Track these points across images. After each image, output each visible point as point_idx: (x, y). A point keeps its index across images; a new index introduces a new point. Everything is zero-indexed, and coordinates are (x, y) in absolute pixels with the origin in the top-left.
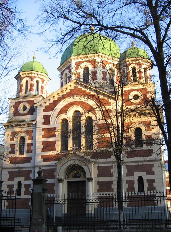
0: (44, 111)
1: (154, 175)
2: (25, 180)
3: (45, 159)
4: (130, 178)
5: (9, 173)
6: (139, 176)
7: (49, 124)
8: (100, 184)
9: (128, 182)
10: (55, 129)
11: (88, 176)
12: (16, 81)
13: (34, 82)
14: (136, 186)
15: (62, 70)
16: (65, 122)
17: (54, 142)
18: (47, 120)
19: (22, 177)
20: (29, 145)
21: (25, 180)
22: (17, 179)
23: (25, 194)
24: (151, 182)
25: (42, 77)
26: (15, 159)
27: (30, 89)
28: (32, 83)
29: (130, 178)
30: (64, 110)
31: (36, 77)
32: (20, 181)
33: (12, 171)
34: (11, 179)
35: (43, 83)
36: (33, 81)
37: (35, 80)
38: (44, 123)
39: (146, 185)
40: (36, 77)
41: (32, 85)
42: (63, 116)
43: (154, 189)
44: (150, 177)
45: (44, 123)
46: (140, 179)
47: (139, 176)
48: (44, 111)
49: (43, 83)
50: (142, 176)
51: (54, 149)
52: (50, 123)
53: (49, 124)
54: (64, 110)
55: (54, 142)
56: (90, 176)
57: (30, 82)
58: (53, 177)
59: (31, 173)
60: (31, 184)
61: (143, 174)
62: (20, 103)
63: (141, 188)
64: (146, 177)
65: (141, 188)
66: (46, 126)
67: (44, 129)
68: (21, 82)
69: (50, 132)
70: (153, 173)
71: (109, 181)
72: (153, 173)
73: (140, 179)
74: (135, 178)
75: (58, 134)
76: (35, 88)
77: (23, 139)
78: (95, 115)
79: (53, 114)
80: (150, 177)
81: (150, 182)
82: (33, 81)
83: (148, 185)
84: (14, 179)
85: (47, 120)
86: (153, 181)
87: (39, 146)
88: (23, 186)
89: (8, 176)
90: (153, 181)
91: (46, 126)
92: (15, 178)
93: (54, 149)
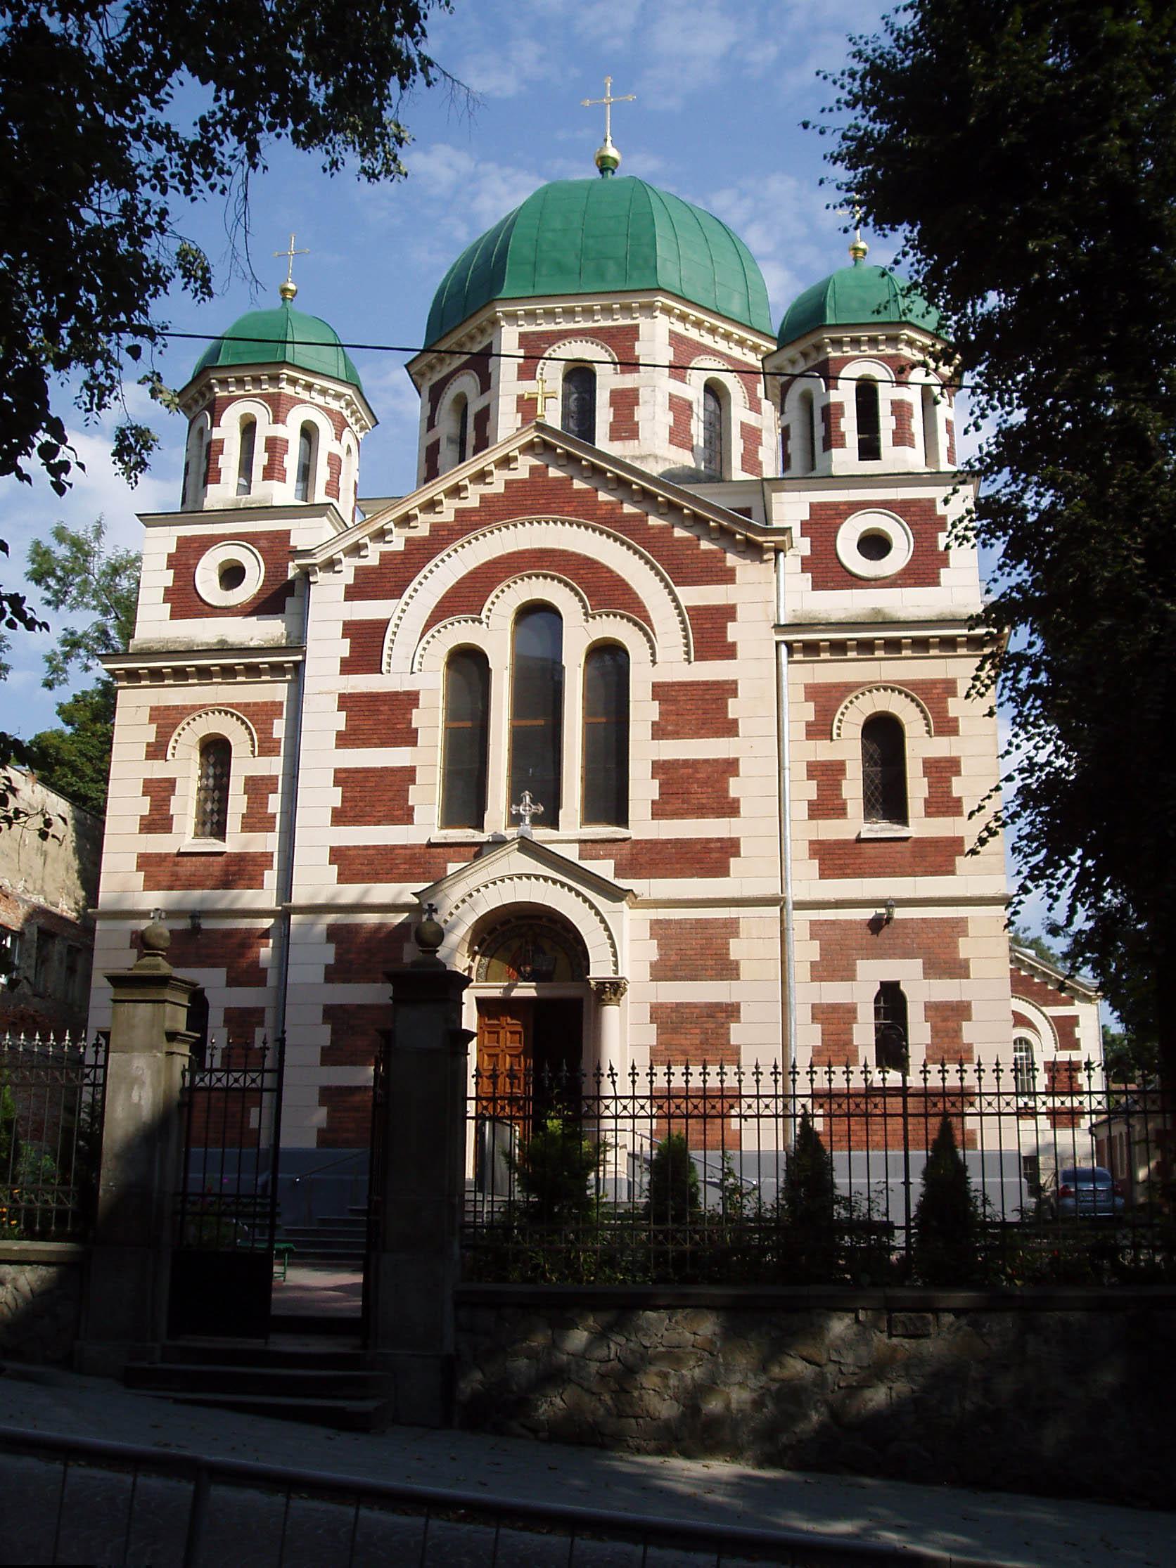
0: (353, 593)
1: (968, 977)
2: (232, 982)
3: (351, 864)
4: (835, 992)
6: (882, 983)
7: (374, 666)
8: (668, 1019)
9: (822, 1013)
10: (411, 699)
11: (599, 969)
12: (182, 420)
13: (290, 431)
14: (864, 1036)
15: (437, 377)
16: (468, 665)
17: (408, 775)
18: (366, 645)
20: (258, 787)
21: (232, 982)
24: (949, 1016)
25: (335, 405)
27: (265, 468)
28: (279, 431)
29: (835, 992)
30: (466, 598)
31: (303, 402)
35: (339, 437)
36: (284, 422)
37: (297, 417)
38: (348, 667)
39: (919, 1034)
40: (303, 402)
41: (274, 446)
42: (460, 632)
43: (962, 1056)
44: (946, 990)
45: (348, 667)
46: (891, 1000)
47: (882, 983)
48: (353, 593)
49: (339, 437)
50: (897, 984)
51: (406, 816)
52: (384, 668)
53: (374, 666)
54: (466, 598)
55: (408, 775)
56: (616, 972)
57: (265, 430)
60: (262, 1010)
61: (907, 972)
62: (207, 543)
63: (892, 1050)
64: (920, 992)
65: (892, 1050)
67: (345, 701)
68: (216, 423)
69: (378, 718)
70: (959, 970)
71: (718, 1005)
72: (959, 970)
73: (891, 1000)
74: (860, 993)
75: (431, 720)
76: (292, 462)
77: (216, 751)
78: (646, 634)
79: (406, 614)
80: (946, 990)
81: (945, 1020)
82: (284, 422)
83: (935, 1031)
85: (366, 645)
86: (961, 1011)
88: (215, 1018)
90: (961, 1011)
93: (406, 816)
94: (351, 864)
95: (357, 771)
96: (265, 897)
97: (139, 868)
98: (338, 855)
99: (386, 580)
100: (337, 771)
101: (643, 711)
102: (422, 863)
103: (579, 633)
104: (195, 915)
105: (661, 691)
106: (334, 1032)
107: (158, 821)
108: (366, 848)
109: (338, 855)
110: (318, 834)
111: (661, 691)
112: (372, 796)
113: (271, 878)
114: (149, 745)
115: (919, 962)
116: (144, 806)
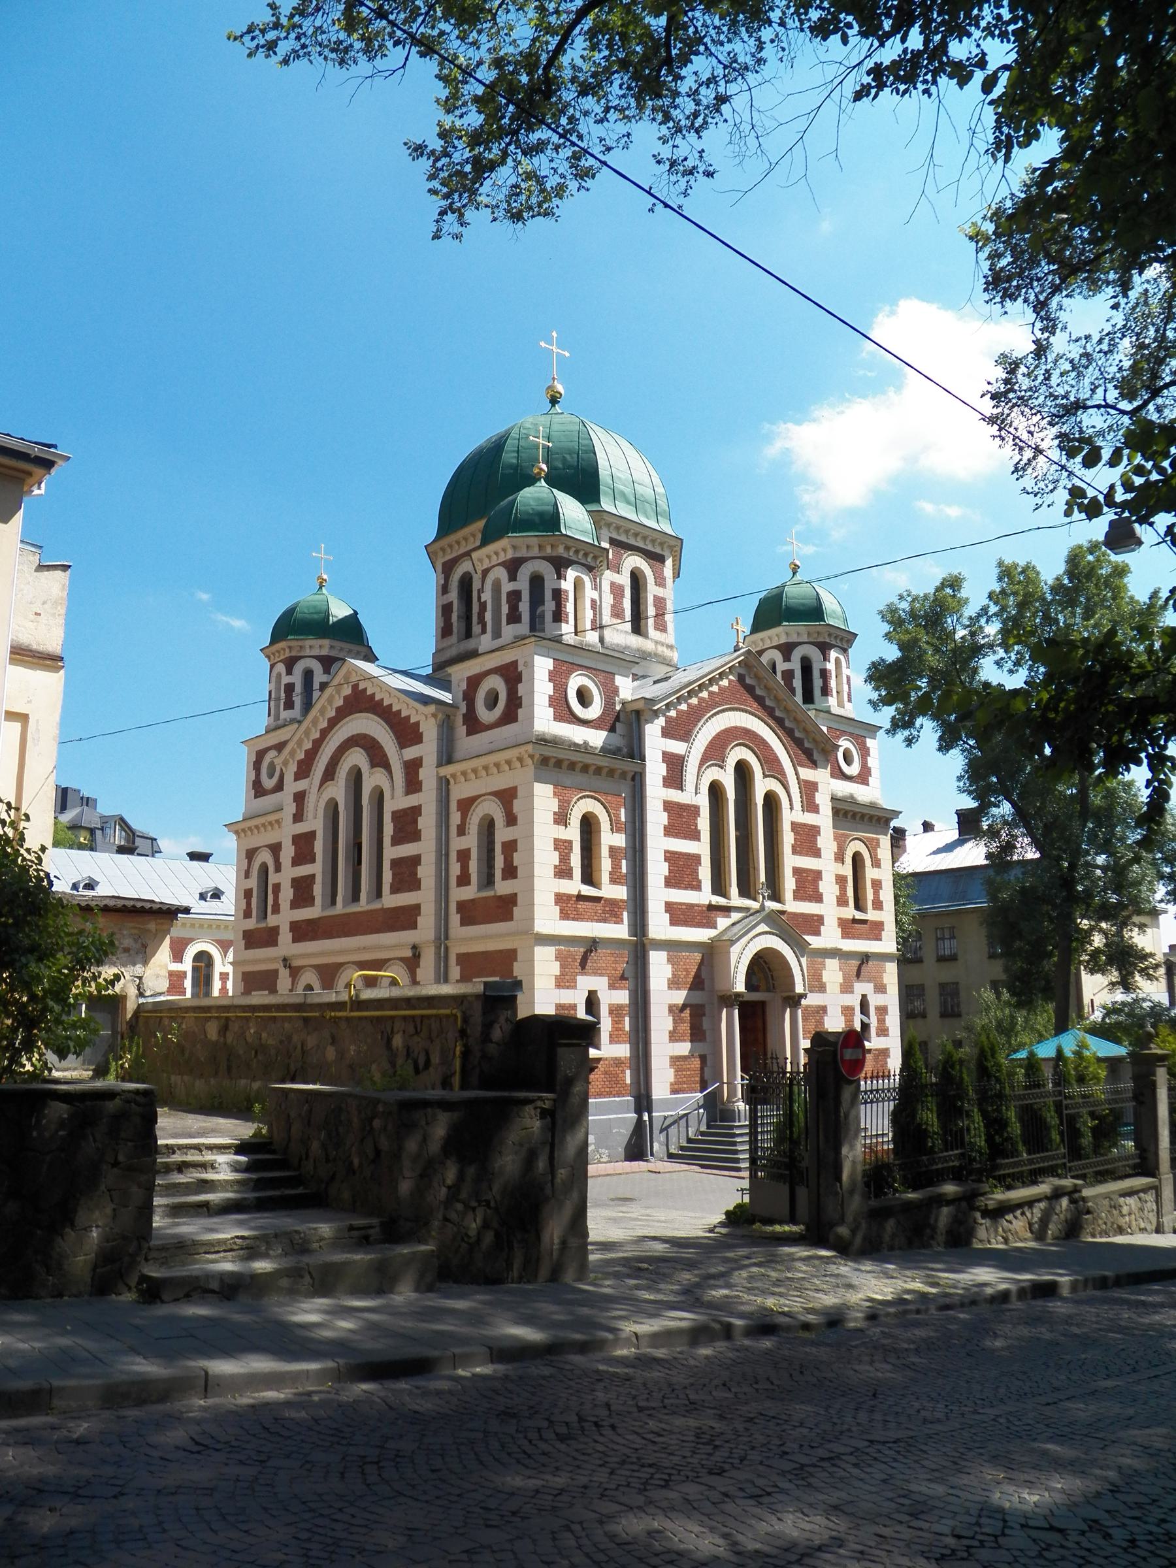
3: (679, 915)
19: (601, 975)
42: (712, 774)
51: (698, 887)
64: (874, 1000)
66: (674, 795)
67: (669, 806)
69: (681, 820)
74: (854, 1001)
89: (555, 968)
91: (674, 795)
92: (579, 978)
94: (679, 915)
95: (676, 853)
98: (670, 907)
99: (680, 729)
100: (666, 852)
101: (788, 838)
103: (762, 785)
105: (795, 826)
107: (563, 872)
109: (670, 907)
111: (795, 826)
112: (681, 871)
114: (555, 813)
115: (872, 985)
116: (555, 858)
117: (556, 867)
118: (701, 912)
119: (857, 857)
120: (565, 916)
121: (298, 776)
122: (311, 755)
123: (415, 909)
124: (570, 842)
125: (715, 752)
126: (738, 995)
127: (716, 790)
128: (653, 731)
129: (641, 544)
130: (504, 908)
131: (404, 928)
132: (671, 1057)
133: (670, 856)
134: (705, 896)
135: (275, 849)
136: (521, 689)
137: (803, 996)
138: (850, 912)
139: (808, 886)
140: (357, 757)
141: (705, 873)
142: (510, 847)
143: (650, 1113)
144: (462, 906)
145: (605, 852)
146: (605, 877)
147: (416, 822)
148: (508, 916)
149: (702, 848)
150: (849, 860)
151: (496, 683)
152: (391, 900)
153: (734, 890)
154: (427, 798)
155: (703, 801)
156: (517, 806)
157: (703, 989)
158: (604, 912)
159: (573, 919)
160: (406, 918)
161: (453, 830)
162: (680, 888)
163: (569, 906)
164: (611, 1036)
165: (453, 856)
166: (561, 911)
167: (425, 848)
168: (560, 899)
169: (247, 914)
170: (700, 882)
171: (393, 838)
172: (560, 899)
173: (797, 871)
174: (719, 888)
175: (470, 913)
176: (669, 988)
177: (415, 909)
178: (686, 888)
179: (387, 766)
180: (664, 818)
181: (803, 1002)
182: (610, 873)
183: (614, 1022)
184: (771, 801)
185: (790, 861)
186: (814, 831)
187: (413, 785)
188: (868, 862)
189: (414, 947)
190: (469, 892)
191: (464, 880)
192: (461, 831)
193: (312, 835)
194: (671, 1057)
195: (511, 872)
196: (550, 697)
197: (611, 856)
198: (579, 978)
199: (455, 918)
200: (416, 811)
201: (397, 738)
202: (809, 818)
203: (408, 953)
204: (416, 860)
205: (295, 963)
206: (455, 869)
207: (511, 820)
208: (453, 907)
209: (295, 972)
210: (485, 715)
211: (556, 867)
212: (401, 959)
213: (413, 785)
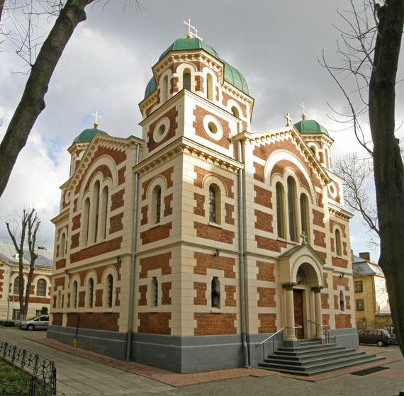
2: (226, 276)
3: (262, 242)
5: (197, 255)
19: (221, 269)
21: (226, 276)
22: (212, 273)
23: (227, 304)
26: (207, 229)
32: (217, 278)
33: (202, 253)
34: (199, 270)
42: (277, 178)
51: (271, 231)
58: (272, 279)
59: (234, 264)
74: (338, 293)
84: (206, 271)
87: (251, 219)
91: (259, 184)
92: (208, 269)
94: (262, 242)
95: (260, 212)
96: (234, 247)
97: (195, 227)
98: (257, 238)
101: (311, 216)
102: (273, 245)
103: (300, 190)
104: (218, 250)
106: (260, 296)
107: (199, 211)
108: (264, 238)
109: (257, 238)
110: (252, 232)
112: (263, 221)
113: (235, 240)
116: (195, 203)
117: (195, 208)
118: (273, 243)
119: (337, 231)
120: (199, 235)
121: (76, 193)
122: (81, 182)
123: (120, 239)
124: (204, 197)
125: (278, 169)
126: (293, 284)
127: (279, 186)
128: (249, 148)
129: (236, 98)
130: (164, 231)
131: (114, 249)
132: (259, 314)
133: (257, 213)
134: (274, 236)
135: (67, 226)
136: (177, 119)
137: (322, 288)
138: (335, 254)
139: (320, 238)
140: (99, 177)
141: (274, 224)
142: (169, 198)
143: (248, 342)
144: (143, 235)
145: (223, 206)
146: (223, 219)
147: (122, 197)
148: (167, 235)
149: (273, 212)
150: (334, 232)
151: (166, 122)
152: (110, 237)
153: (288, 236)
154: (128, 185)
155: (273, 190)
156: (173, 176)
157: (274, 281)
158: (222, 236)
159: (205, 238)
160: (116, 244)
161: (140, 198)
162: (263, 230)
163: (201, 230)
164: (226, 302)
165: (140, 210)
166: (198, 232)
167: (126, 209)
168: (197, 225)
169: (57, 256)
170: (272, 228)
171: (111, 208)
172: (197, 225)
173: (315, 232)
174: (281, 233)
175: (146, 237)
176: (258, 279)
177: (120, 239)
178: (266, 230)
179: (110, 175)
180: (254, 194)
181: (322, 291)
182: (226, 217)
183: (228, 295)
184: (303, 196)
185: (313, 227)
186: (322, 215)
187: (122, 180)
188: (341, 234)
189: (118, 257)
190: (146, 228)
191: (144, 221)
192: (144, 197)
193: (80, 215)
194: (259, 314)
195: (169, 211)
196: (194, 122)
197: (226, 208)
198: (208, 269)
199: (140, 241)
200: (122, 192)
201: (116, 161)
202: (319, 209)
203: (116, 261)
204: (121, 215)
205: (71, 272)
206: (141, 217)
207: (170, 184)
208: (139, 236)
209: (71, 276)
210: (157, 138)
211: (195, 208)
212: (113, 264)
213: (122, 180)
